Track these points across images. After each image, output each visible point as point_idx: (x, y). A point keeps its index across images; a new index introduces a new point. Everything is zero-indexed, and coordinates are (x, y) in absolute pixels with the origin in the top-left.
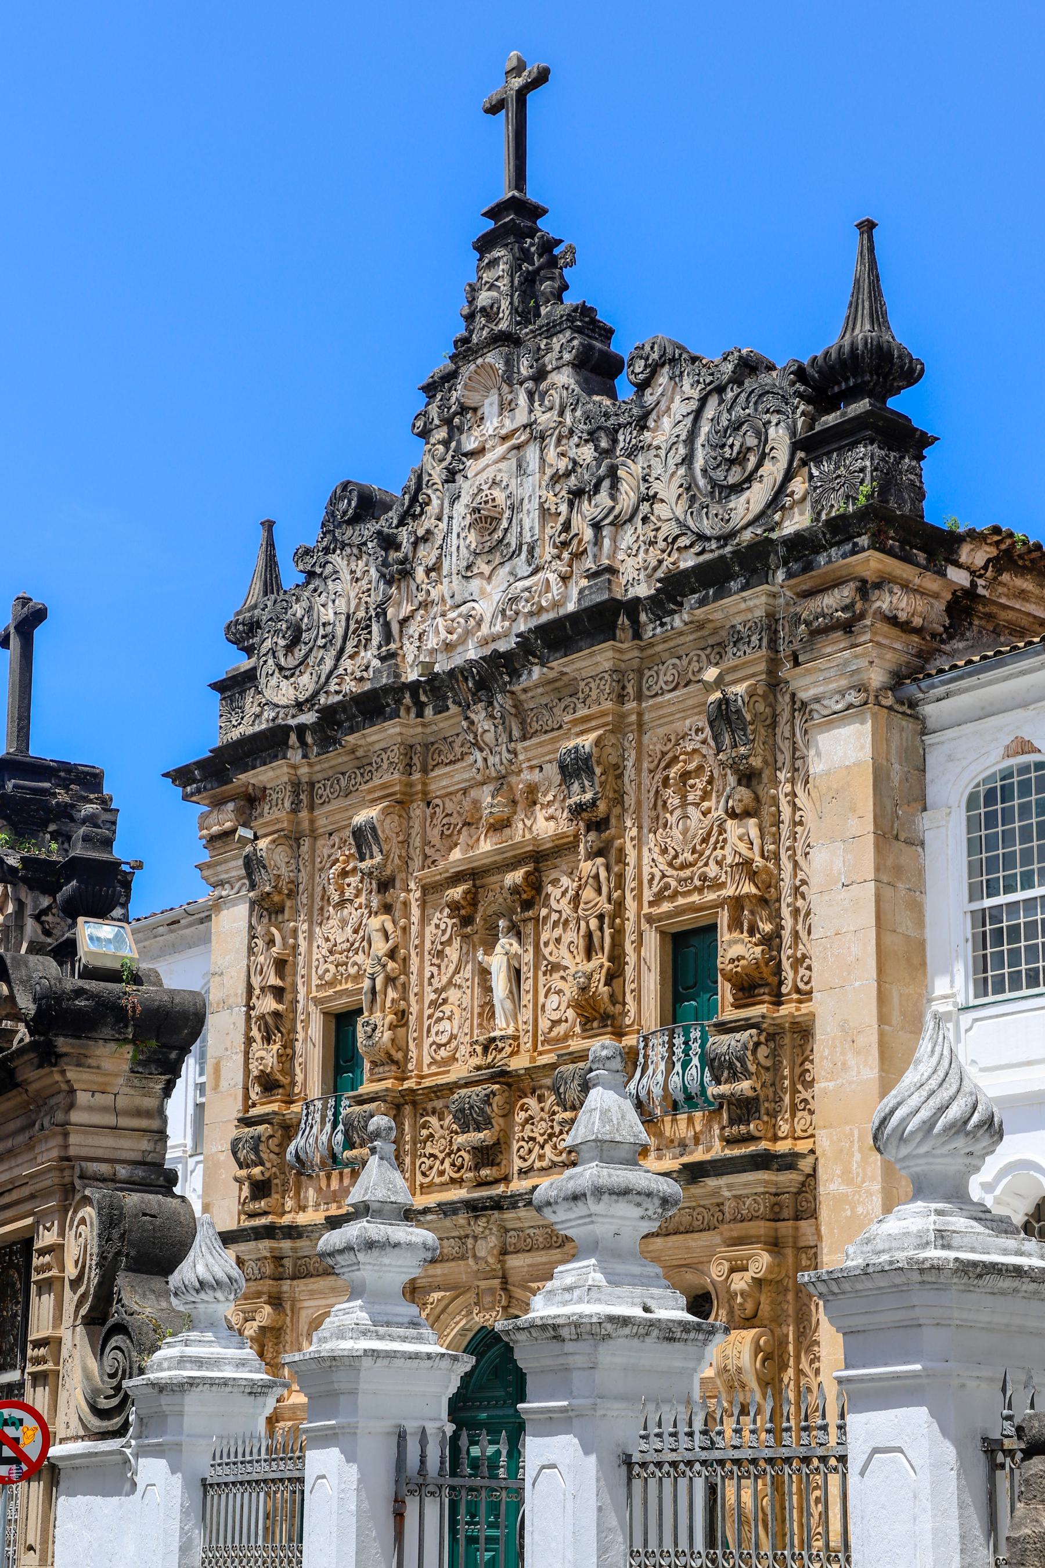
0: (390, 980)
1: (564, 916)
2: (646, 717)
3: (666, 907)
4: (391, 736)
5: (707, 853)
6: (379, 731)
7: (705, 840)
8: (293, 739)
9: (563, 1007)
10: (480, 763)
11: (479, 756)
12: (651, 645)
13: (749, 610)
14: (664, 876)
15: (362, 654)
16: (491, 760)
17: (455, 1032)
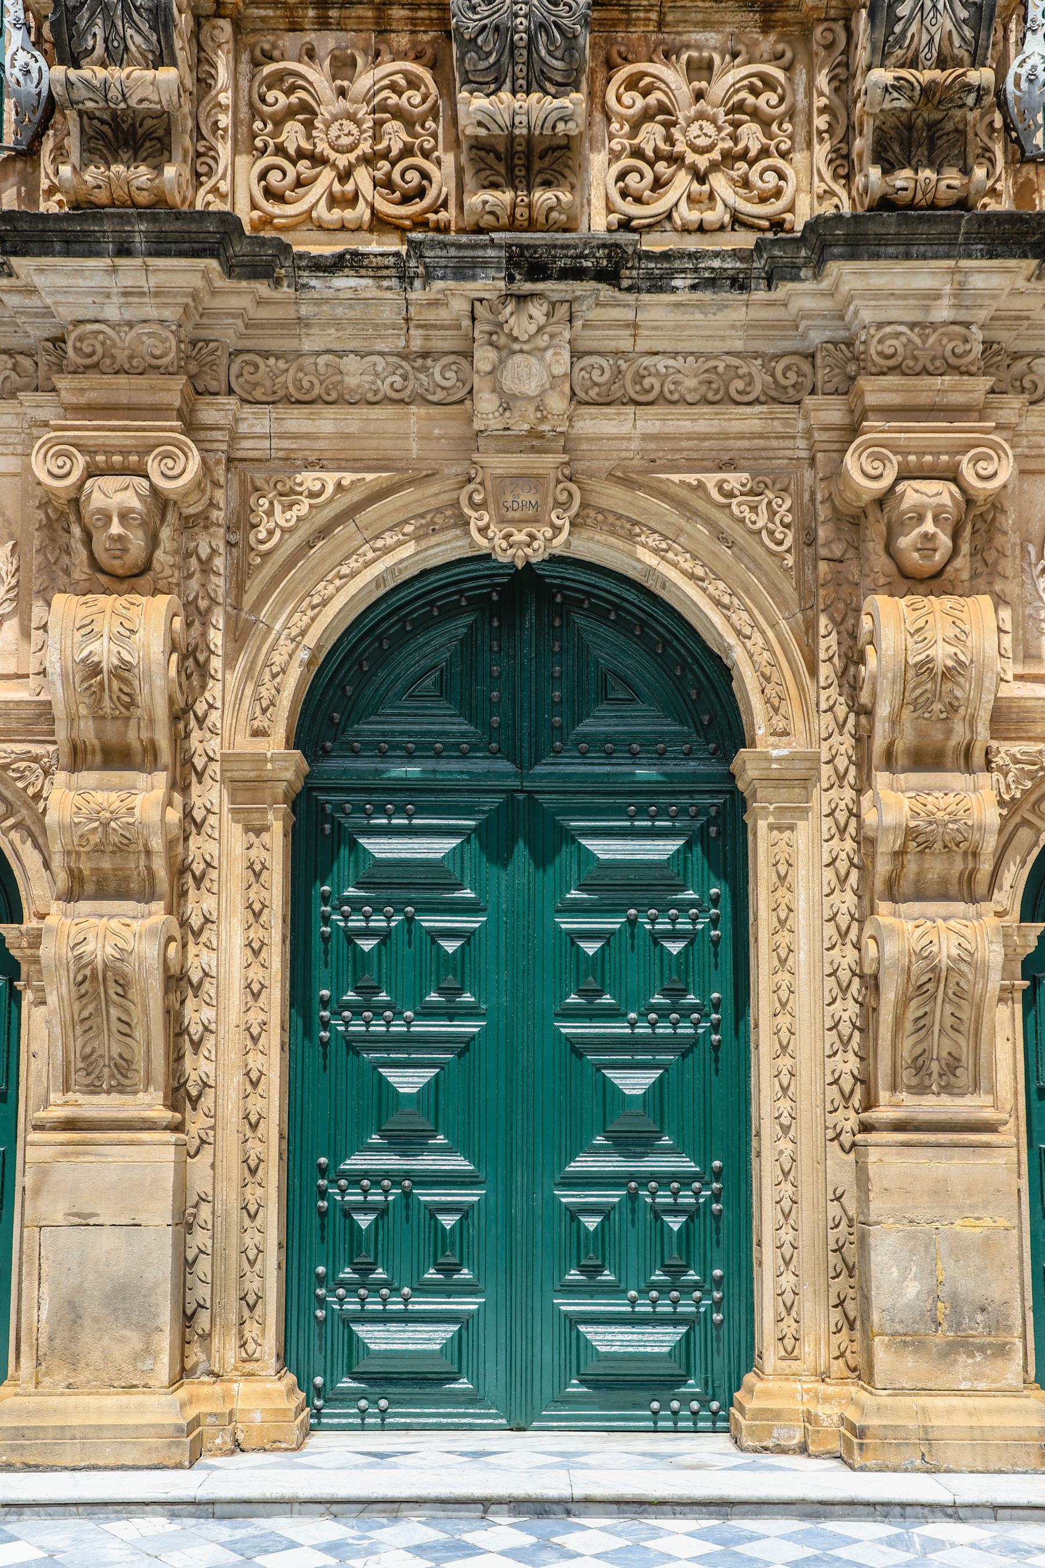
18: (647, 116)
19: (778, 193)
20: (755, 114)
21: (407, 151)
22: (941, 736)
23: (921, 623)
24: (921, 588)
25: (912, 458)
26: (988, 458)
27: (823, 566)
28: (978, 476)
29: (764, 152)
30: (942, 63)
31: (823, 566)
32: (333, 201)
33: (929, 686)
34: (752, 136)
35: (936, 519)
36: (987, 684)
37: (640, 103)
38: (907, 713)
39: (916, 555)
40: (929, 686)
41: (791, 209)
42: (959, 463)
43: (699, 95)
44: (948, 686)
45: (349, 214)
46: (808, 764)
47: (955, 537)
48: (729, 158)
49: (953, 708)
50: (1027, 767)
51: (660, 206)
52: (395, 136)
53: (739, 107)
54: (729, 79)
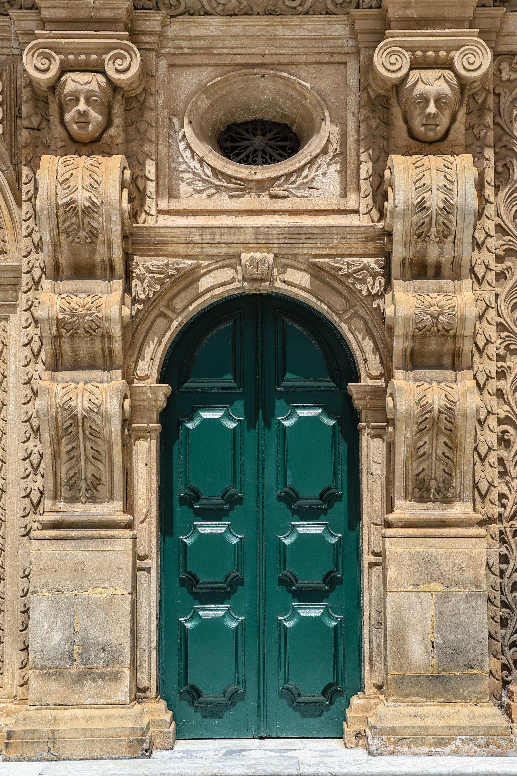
22: (87, 255)
23: (67, 175)
24: (84, 150)
25: (71, 57)
26: (122, 57)
27: (25, 134)
28: (116, 70)
31: (25, 134)
33: (74, 220)
35: (88, 101)
36: (113, 218)
38: (63, 237)
39: (75, 126)
40: (74, 220)
42: (104, 60)
44: (87, 220)
46: (14, 274)
49: (93, 235)
50: (157, 276)
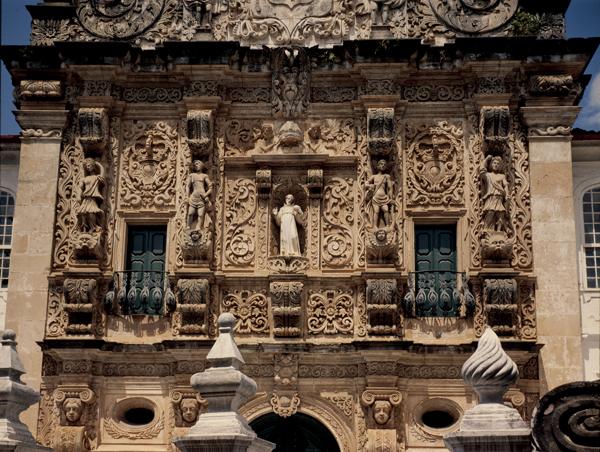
0: (207, 211)
1: (343, 201)
2: (408, 110)
3: (419, 209)
4: (212, 75)
5: (452, 188)
6: (205, 69)
7: (451, 181)
8: (128, 56)
9: (342, 250)
10: (280, 106)
11: (280, 102)
12: (417, 74)
13: (499, 72)
14: (420, 193)
15: (174, 24)
16: (289, 107)
17: (252, 250)
18: (318, 306)
19: (349, 326)
20: (344, 306)
21: (260, 315)
29: (346, 316)
30: (385, 303)
32: (242, 327)
34: (343, 311)
37: (316, 303)
41: (353, 329)
43: (330, 302)
45: (245, 331)
47: (389, 414)
48: (337, 317)
51: (321, 329)
52: (257, 312)
53: (340, 305)
54: (337, 298)
